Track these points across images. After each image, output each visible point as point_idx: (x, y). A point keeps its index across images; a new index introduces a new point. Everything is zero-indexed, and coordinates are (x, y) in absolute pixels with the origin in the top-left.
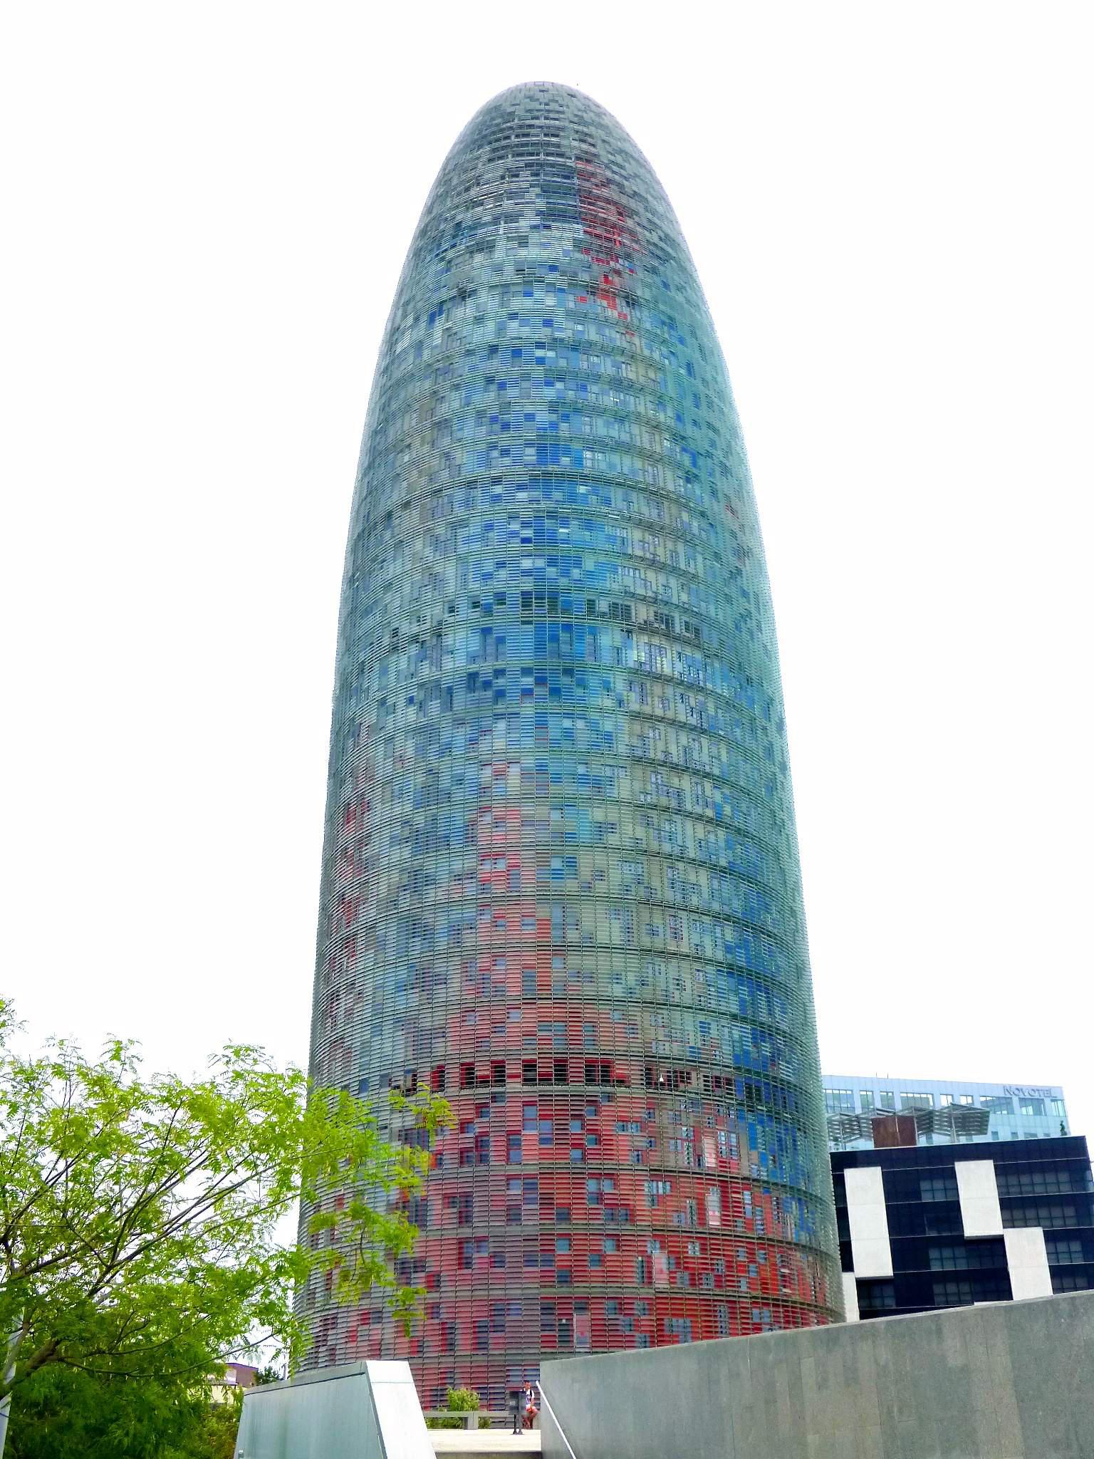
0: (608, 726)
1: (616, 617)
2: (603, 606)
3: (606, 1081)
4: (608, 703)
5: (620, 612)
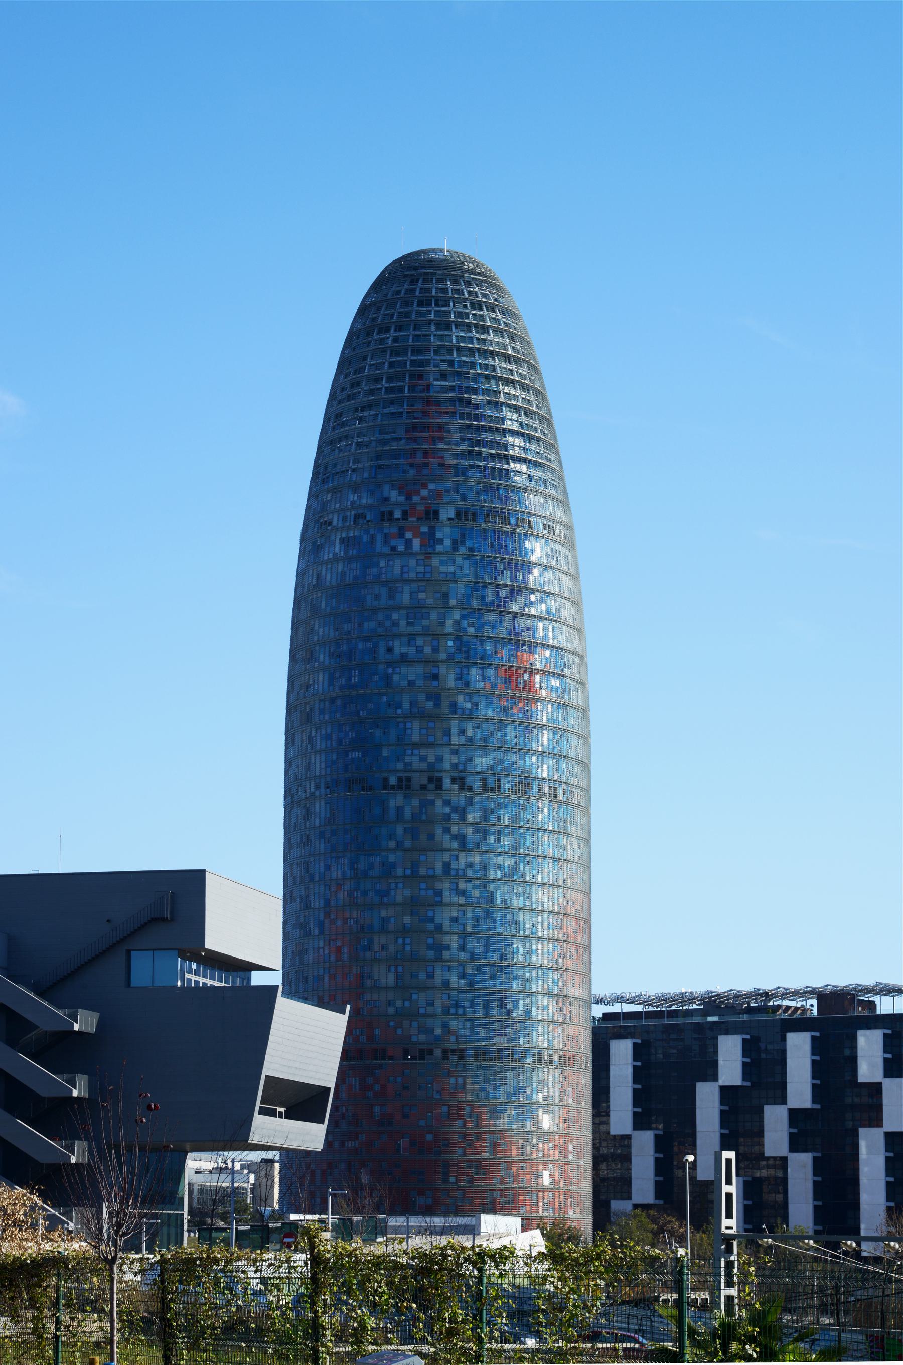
0: (392, 858)
1: (400, 788)
2: (393, 781)
3: (383, 1058)
4: (392, 844)
5: (405, 784)
